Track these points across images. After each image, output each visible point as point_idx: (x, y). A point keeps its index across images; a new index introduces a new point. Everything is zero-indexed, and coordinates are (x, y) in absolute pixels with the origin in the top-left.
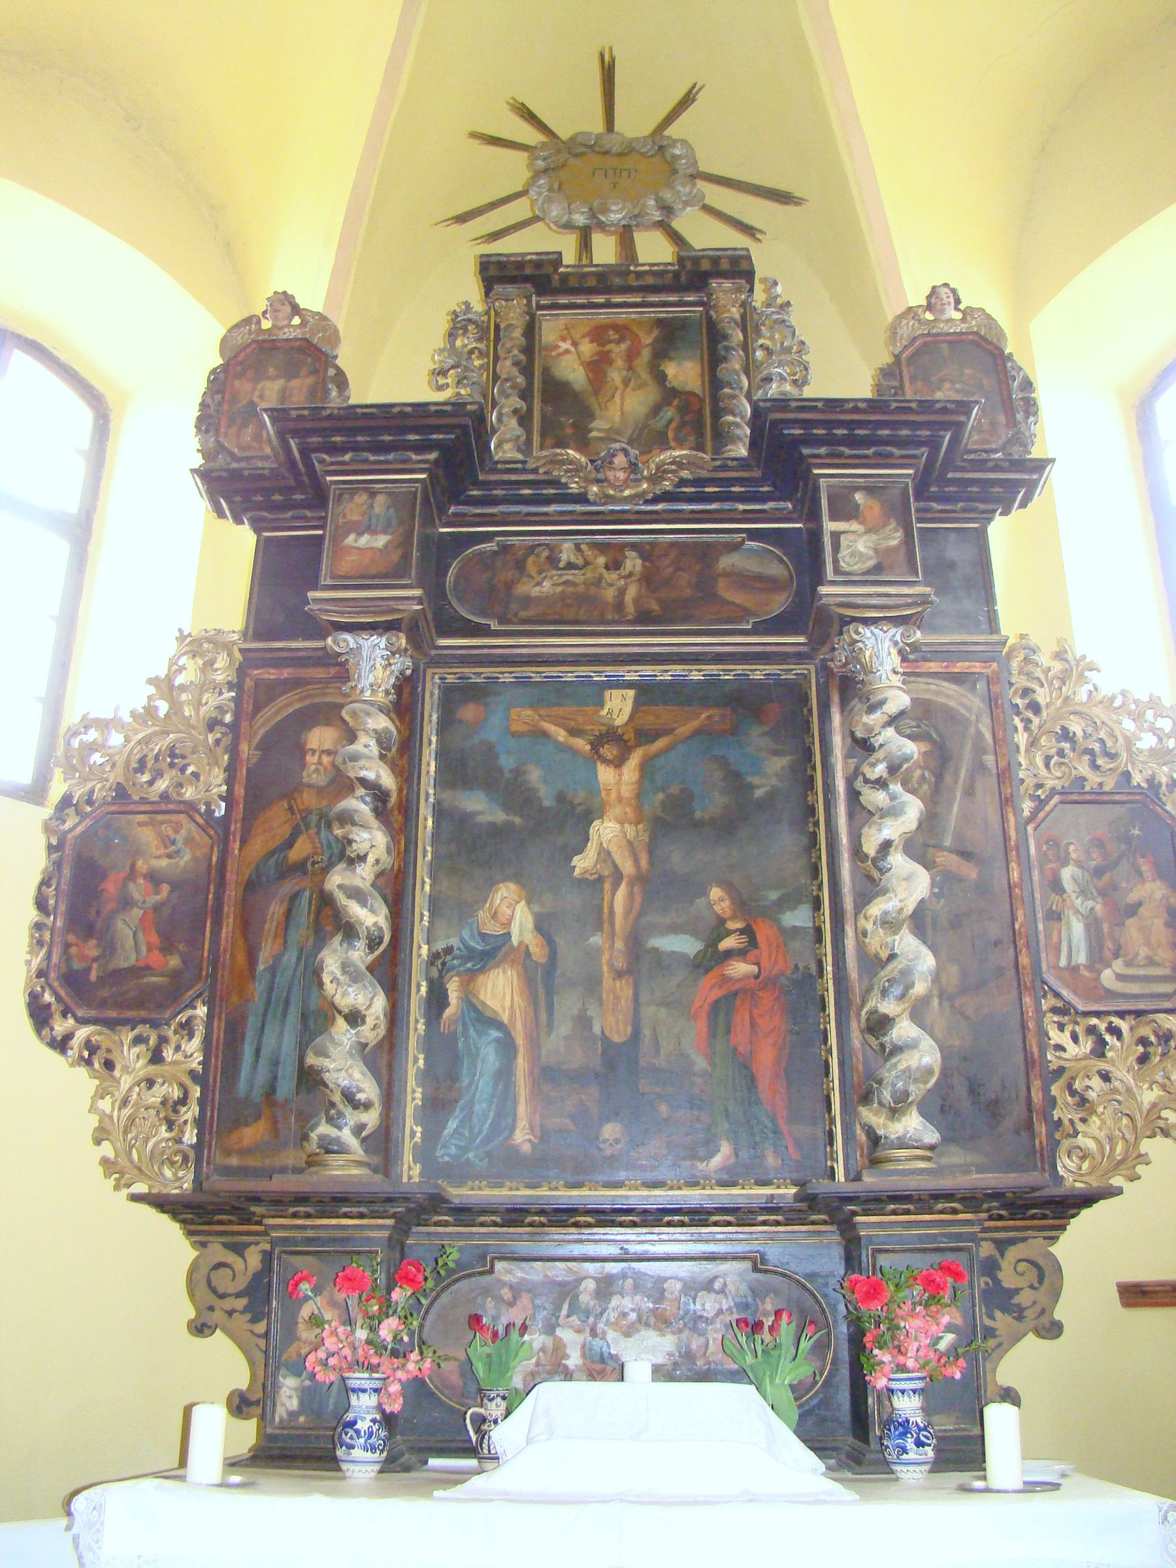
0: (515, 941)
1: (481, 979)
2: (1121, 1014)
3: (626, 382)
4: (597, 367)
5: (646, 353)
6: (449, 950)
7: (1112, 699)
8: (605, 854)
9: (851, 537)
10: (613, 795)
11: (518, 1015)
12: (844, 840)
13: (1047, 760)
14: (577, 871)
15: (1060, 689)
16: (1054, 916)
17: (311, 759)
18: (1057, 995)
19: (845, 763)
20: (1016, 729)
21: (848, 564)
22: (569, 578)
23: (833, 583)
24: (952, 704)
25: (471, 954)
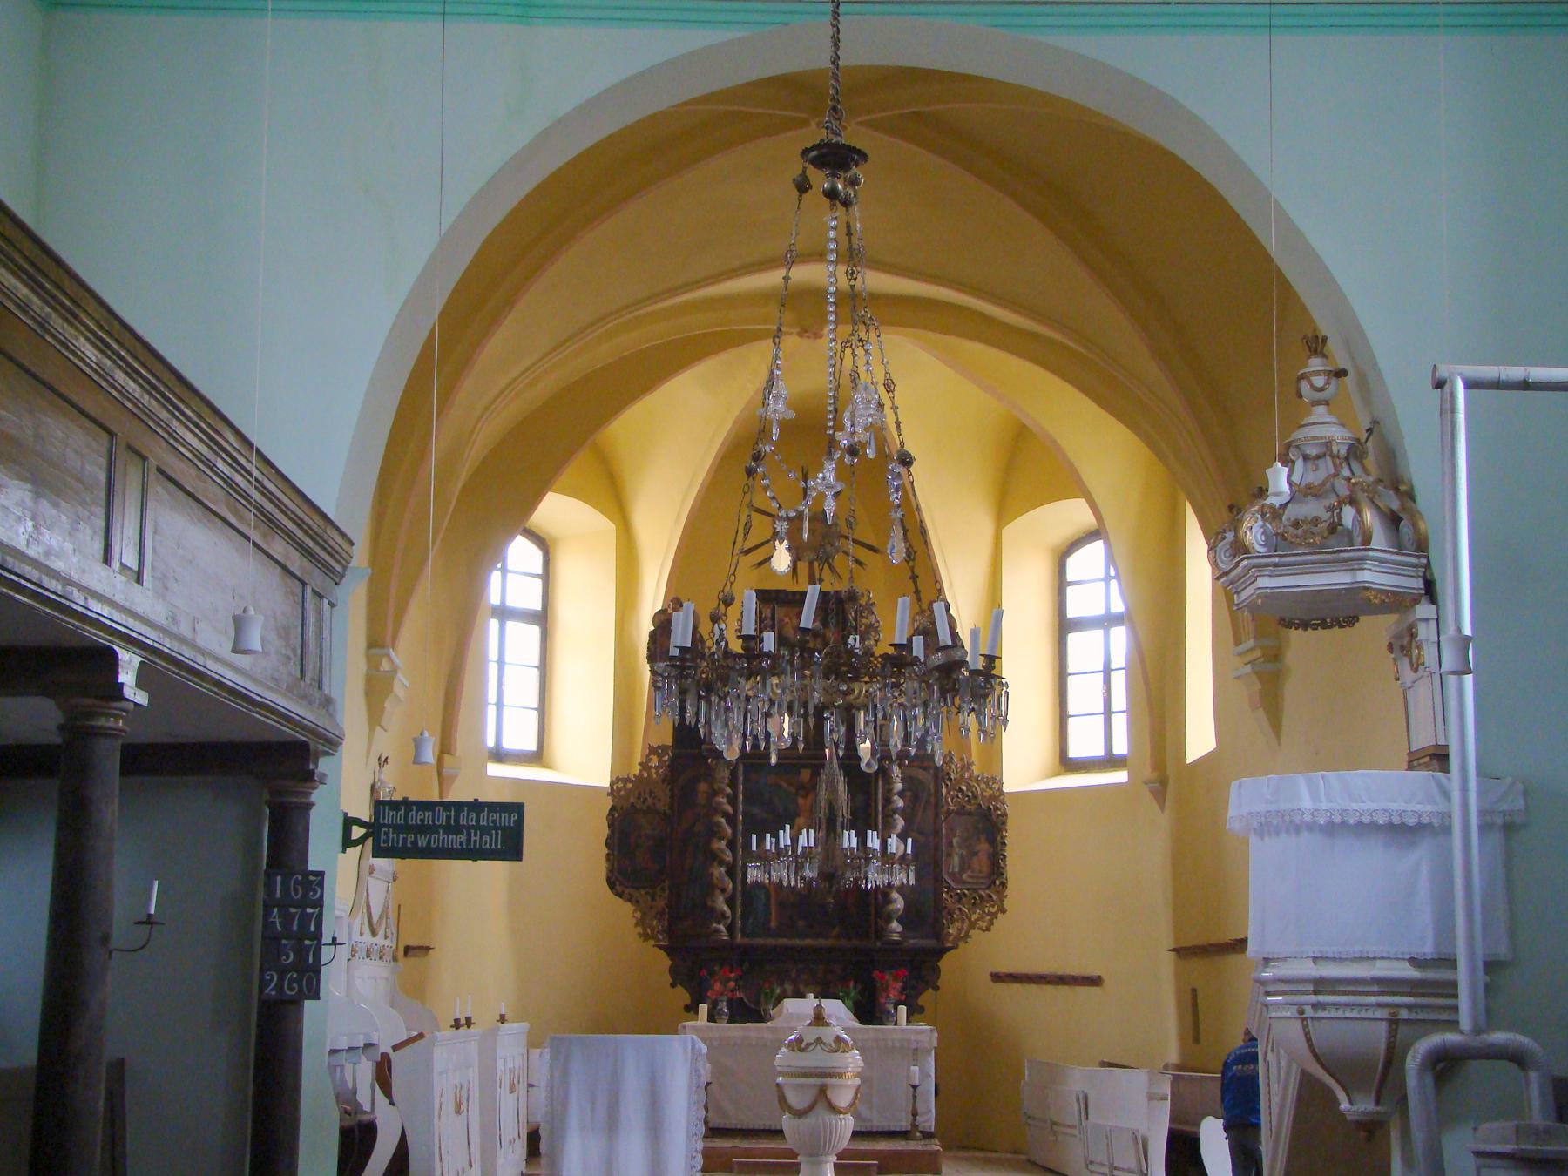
2: (967, 889)
18: (947, 883)
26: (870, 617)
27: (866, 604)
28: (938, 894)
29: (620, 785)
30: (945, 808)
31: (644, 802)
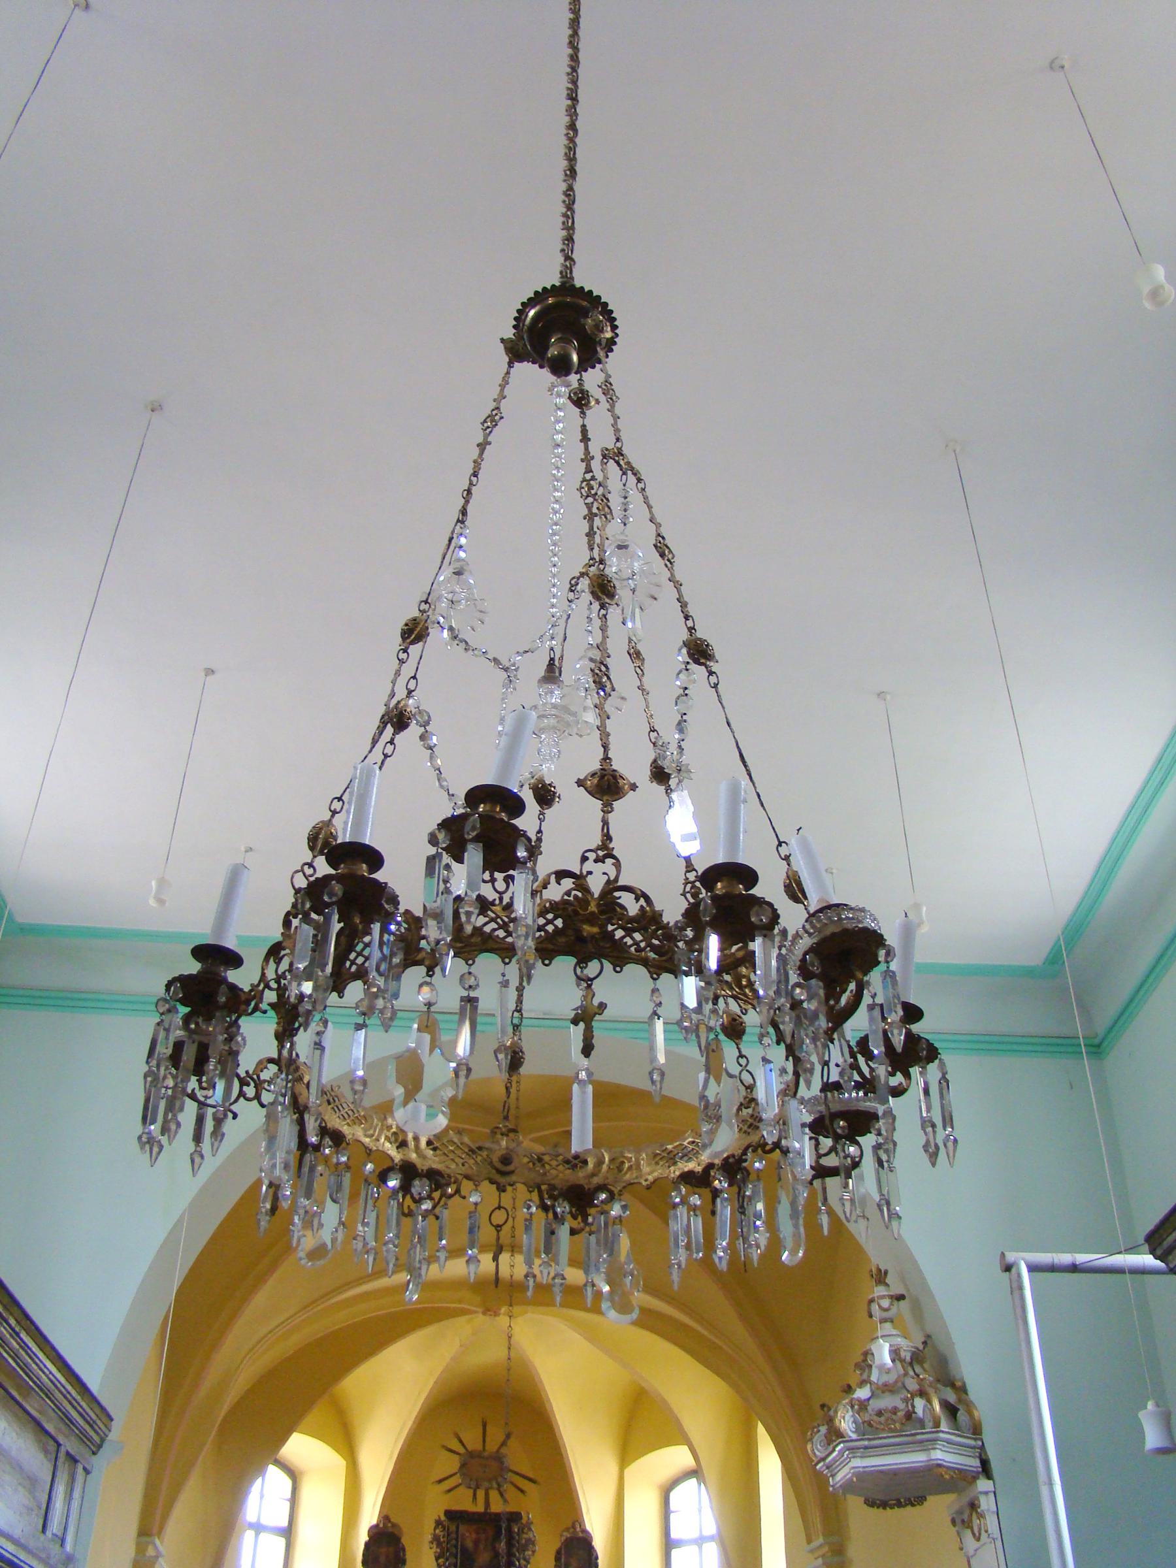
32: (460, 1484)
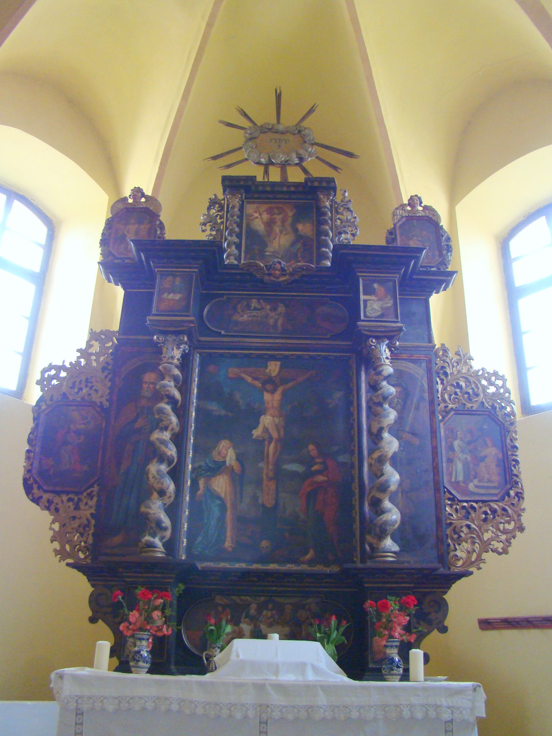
0: (228, 464)
1: (213, 479)
2: (476, 502)
3: (281, 232)
4: (269, 224)
5: (290, 220)
6: (200, 467)
7: (478, 371)
8: (266, 430)
9: (371, 302)
10: (270, 405)
11: (228, 494)
12: (365, 427)
13: (450, 395)
14: (254, 437)
15: (456, 367)
16: (450, 461)
17: (145, 386)
18: (450, 493)
19: (367, 396)
20: (437, 384)
21: (370, 314)
22: (255, 314)
23: (363, 321)
24: (411, 372)
25: (209, 469)
26: (345, 213)
27: (342, 201)
28: (439, 507)
29: (53, 372)
30: (442, 405)
31: (77, 393)
32: (246, 160)
